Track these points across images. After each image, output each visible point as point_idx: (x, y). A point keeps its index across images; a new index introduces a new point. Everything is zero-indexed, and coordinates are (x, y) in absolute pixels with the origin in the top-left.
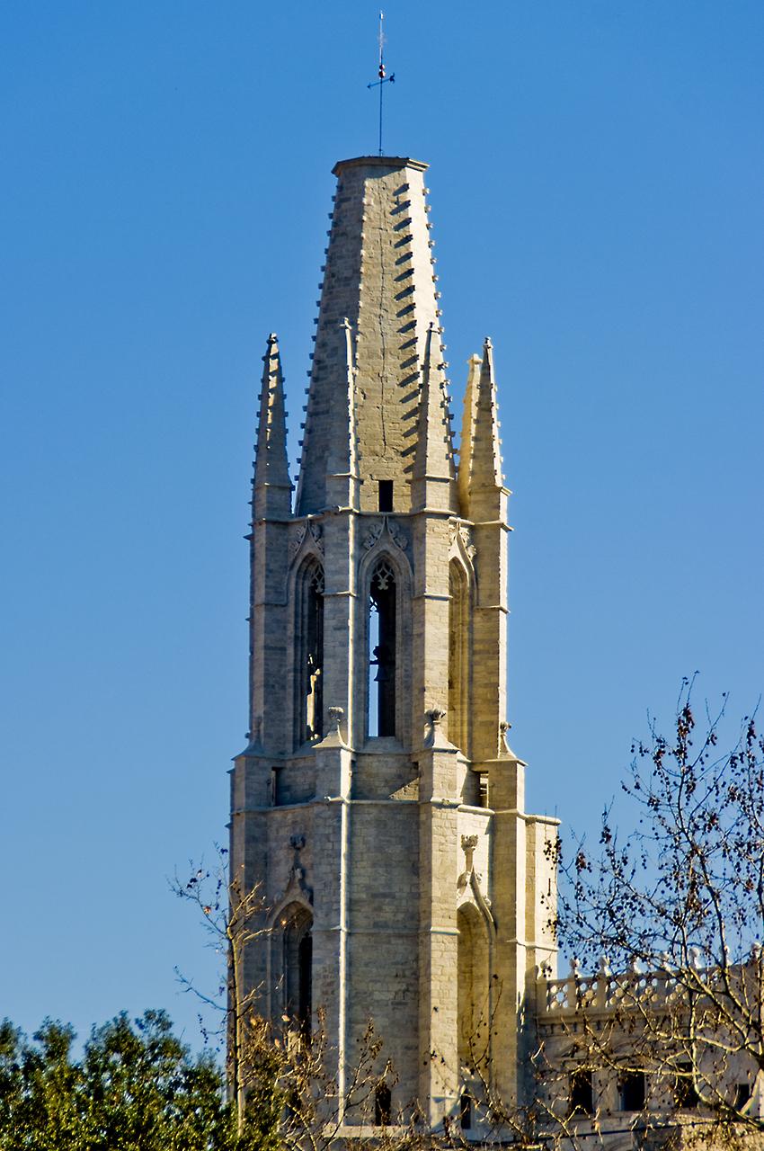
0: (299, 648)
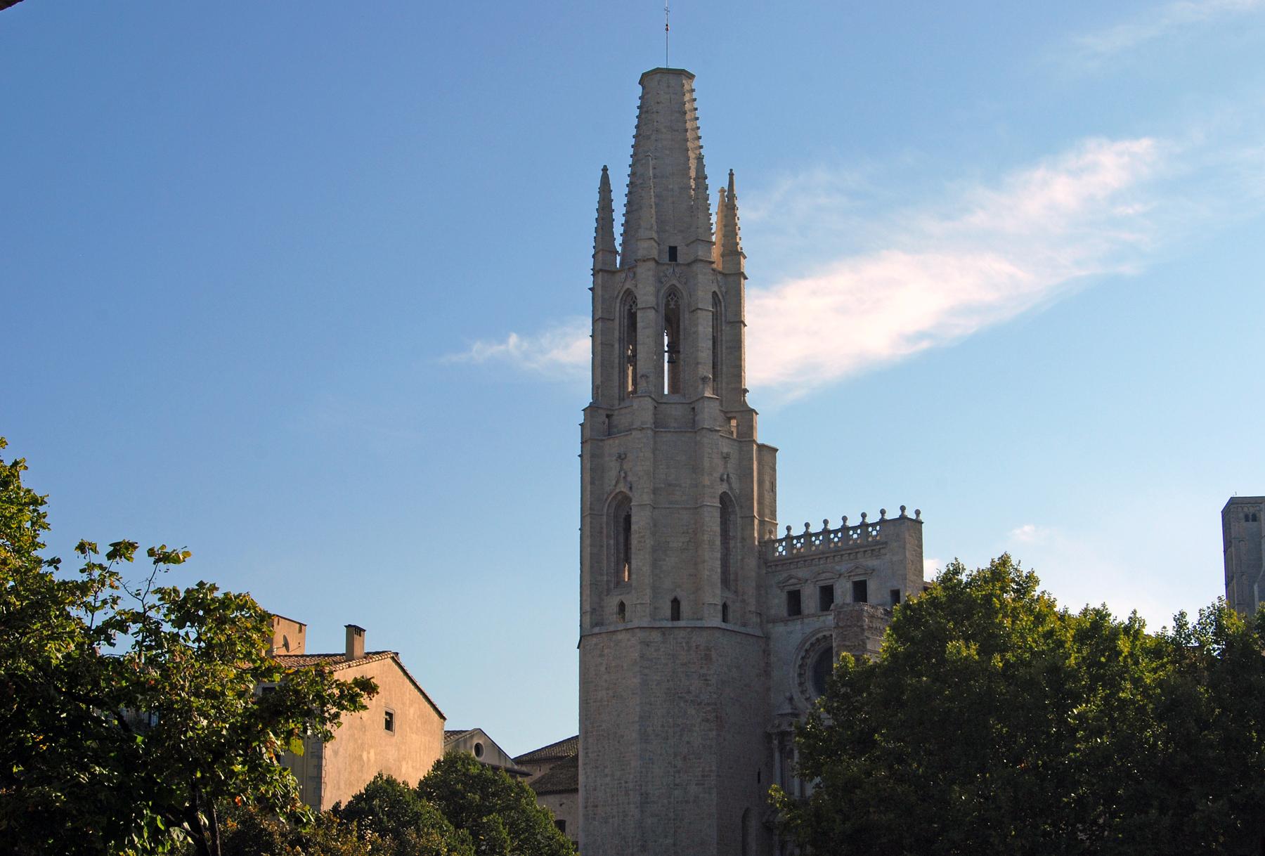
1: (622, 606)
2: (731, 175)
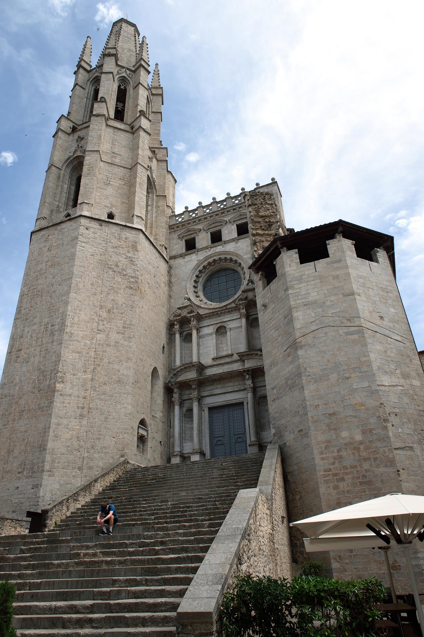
0: (88, 101)
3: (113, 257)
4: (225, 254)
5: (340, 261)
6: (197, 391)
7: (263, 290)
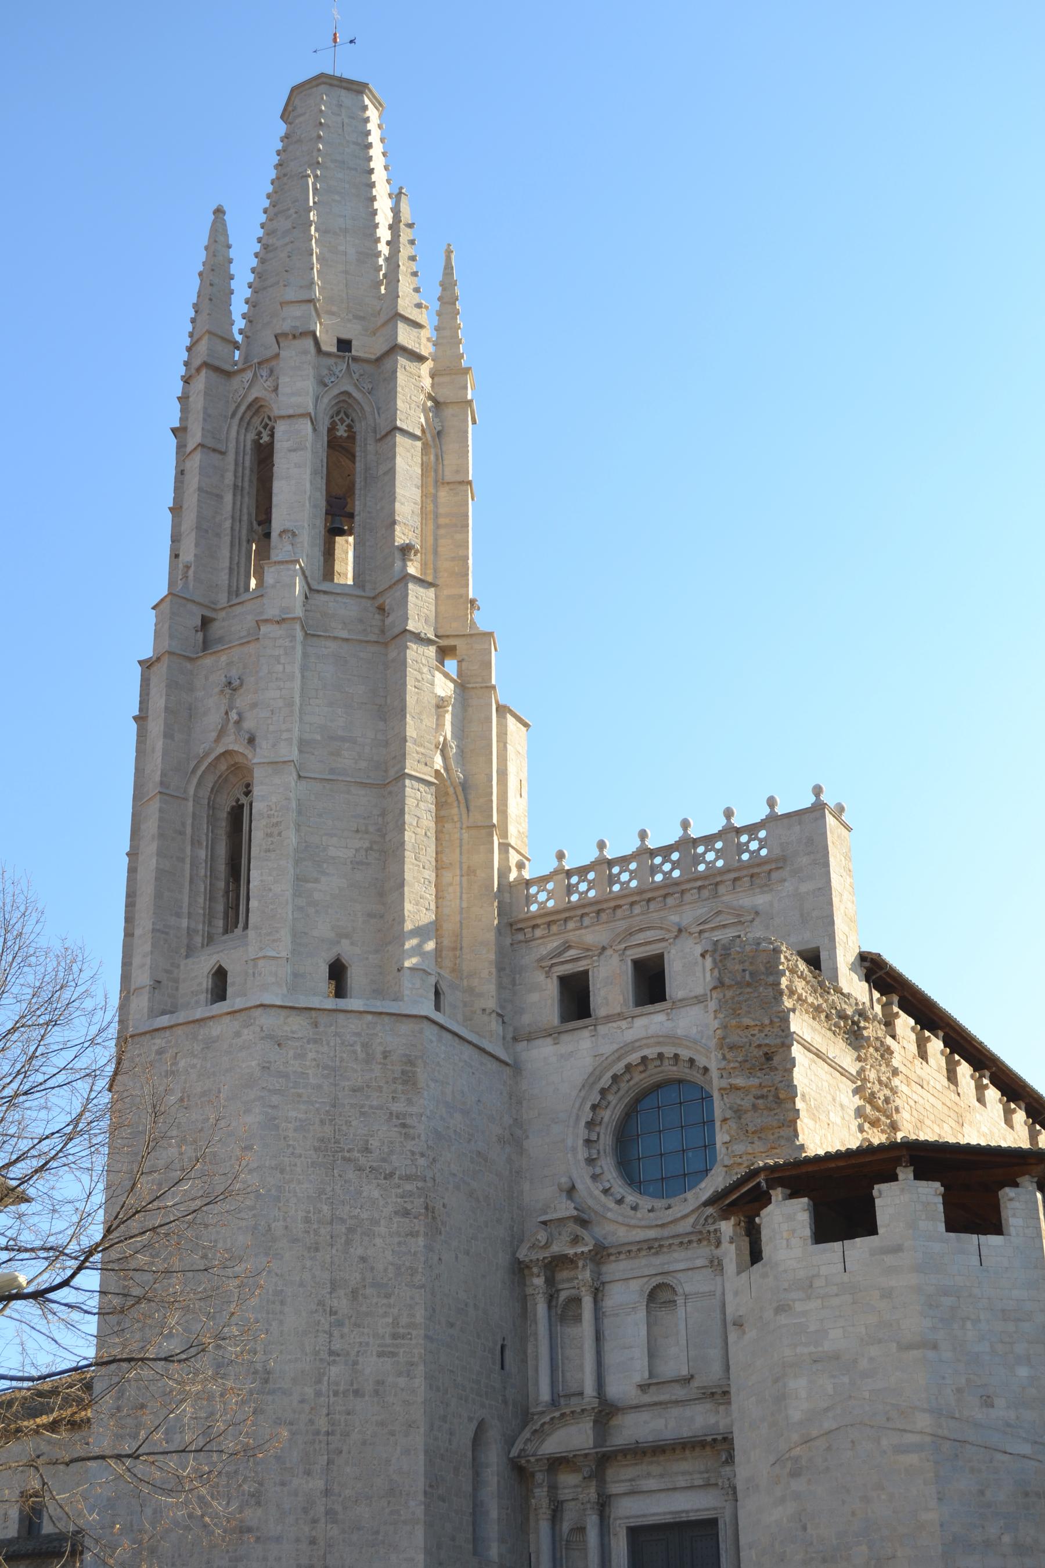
0: (239, 497)
1: (220, 975)
2: (449, 253)
3: (354, 1123)
4: (674, 1045)
5: (898, 1249)
6: (594, 1483)
7: (739, 1273)
